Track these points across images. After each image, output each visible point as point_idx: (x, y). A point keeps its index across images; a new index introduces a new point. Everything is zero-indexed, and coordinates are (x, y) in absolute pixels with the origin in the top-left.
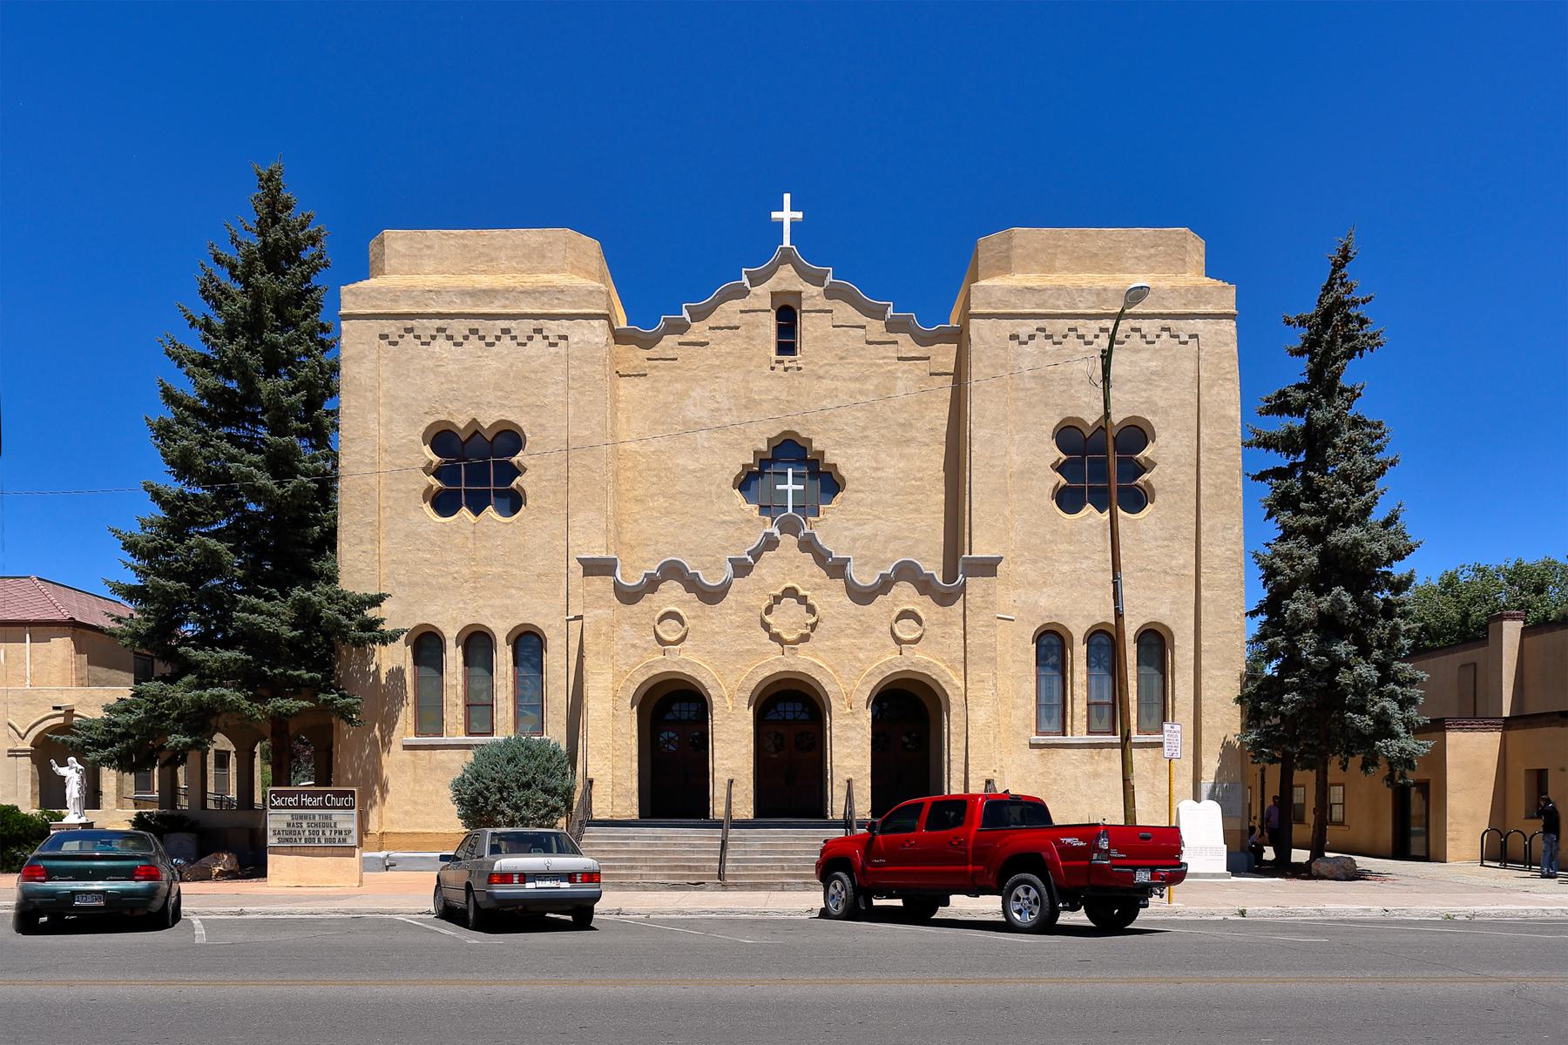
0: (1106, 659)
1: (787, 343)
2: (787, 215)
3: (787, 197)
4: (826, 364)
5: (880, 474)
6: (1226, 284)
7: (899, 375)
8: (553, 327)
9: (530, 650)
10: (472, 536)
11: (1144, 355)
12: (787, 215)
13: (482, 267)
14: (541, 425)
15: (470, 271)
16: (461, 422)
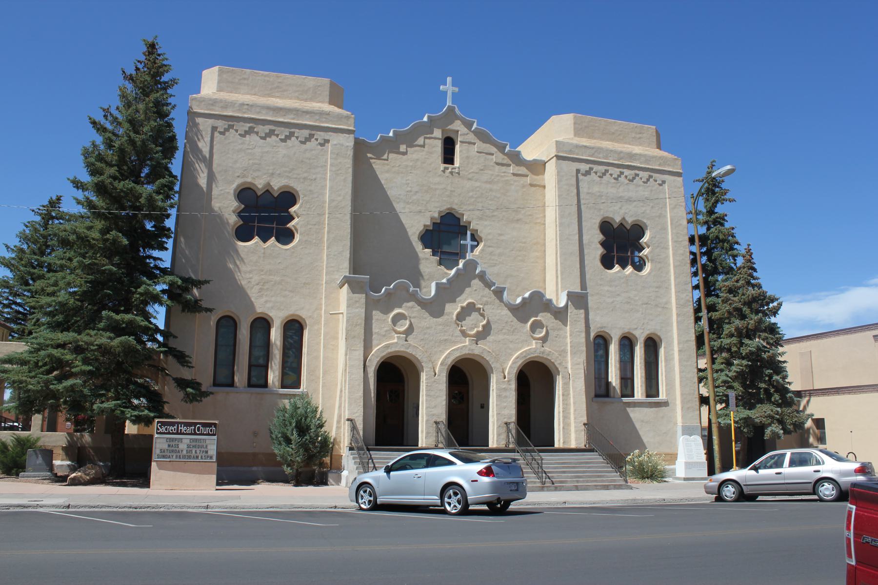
0: (628, 353)
1: (448, 157)
2: (449, 87)
3: (449, 79)
4: (473, 172)
5: (502, 238)
6: (676, 157)
7: (512, 182)
8: (321, 135)
9: (293, 332)
10: (262, 255)
11: (641, 188)
12: (449, 87)
13: (277, 94)
14: (310, 191)
15: (270, 96)
16: (260, 184)
